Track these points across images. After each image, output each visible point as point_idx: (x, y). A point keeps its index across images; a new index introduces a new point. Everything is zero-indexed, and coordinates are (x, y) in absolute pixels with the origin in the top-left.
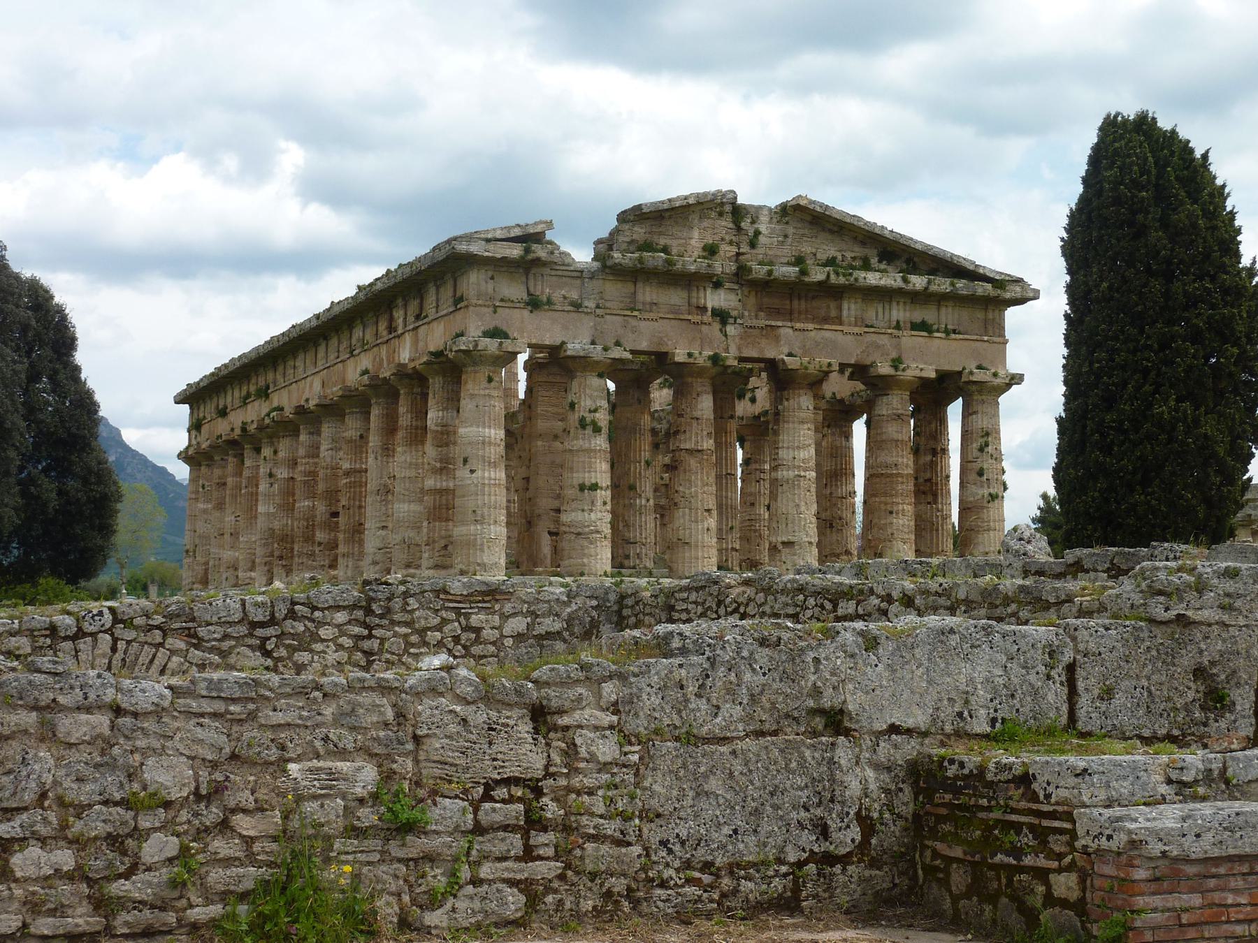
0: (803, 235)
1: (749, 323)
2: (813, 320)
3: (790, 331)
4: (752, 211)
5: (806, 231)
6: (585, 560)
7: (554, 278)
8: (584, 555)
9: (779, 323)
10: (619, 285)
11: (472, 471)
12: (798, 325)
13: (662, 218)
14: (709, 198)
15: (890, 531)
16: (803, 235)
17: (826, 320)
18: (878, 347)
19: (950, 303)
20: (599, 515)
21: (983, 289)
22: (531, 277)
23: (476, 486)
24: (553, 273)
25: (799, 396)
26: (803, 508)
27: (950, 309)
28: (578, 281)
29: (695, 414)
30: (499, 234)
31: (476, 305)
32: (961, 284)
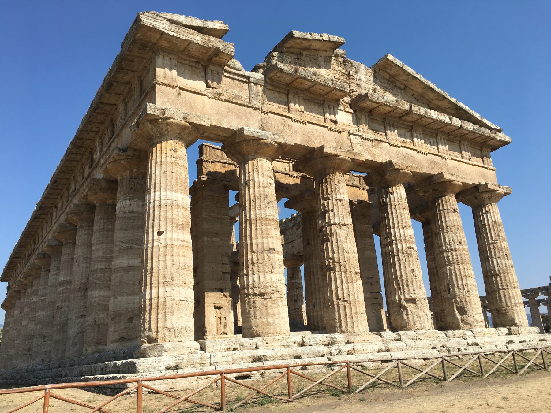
1: (364, 135)
6: (270, 320)
7: (228, 79)
8: (268, 314)
11: (160, 233)
18: (436, 164)
19: (465, 143)
21: (487, 132)
22: (209, 72)
23: (166, 247)
24: (226, 74)
26: (416, 272)
28: (246, 85)
29: (339, 197)
31: (162, 84)
32: (476, 127)
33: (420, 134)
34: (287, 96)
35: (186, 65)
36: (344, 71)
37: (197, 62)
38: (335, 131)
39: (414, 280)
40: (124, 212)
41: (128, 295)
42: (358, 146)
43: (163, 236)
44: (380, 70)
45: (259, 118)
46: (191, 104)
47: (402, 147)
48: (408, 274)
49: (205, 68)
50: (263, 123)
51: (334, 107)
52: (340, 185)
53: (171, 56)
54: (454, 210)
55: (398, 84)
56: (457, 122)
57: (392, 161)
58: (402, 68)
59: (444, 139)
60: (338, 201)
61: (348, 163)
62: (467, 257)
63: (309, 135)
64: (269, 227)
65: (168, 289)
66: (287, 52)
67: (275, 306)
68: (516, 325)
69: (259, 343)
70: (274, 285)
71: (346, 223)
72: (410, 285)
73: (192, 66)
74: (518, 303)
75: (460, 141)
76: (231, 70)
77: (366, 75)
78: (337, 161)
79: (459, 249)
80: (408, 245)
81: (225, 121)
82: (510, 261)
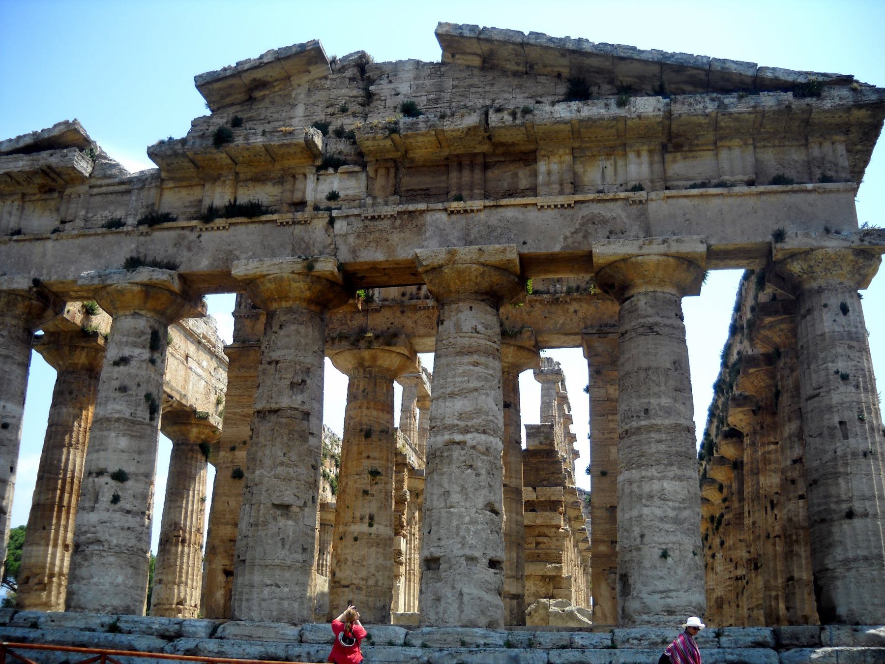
0: (471, 86)
3: (444, 216)
4: (387, 69)
5: (475, 80)
7: (98, 198)
9: (422, 206)
10: (184, 193)
12: (454, 205)
13: (251, 100)
14: (294, 50)
15: (637, 531)
16: (471, 86)
18: (605, 222)
19: (736, 142)
20: (105, 516)
24: (95, 191)
25: (459, 311)
26: (455, 497)
27: (737, 152)
33: (561, 163)
34: (204, 185)
35: (37, 200)
36: (355, 92)
37: (51, 190)
38: (294, 223)
39: (444, 515)
42: (351, 239)
44: (453, 56)
45: (133, 246)
46: (25, 259)
47: (485, 207)
48: (436, 503)
49: (61, 193)
50: (139, 252)
51: (305, 175)
52: (282, 333)
53: (12, 199)
54: (651, 328)
56: (647, 106)
57: (418, 251)
58: (479, 39)
59: (651, 152)
60: (274, 365)
61: (294, 285)
62: (653, 448)
63: (231, 248)
64: (106, 433)
66: (218, 109)
67: (86, 564)
70: (92, 529)
71: (274, 406)
72: (434, 528)
73: (45, 200)
74: (855, 559)
75: (715, 144)
76: (99, 183)
78: (268, 285)
79: (639, 429)
80: (447, 437)
81: (73, 269)
82: (852, 441)
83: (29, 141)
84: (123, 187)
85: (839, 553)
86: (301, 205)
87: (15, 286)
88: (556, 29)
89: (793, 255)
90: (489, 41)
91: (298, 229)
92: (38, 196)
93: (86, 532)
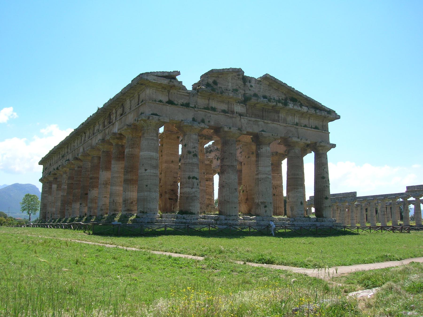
2: (270, 120)
3: (263, 123)
6: (190, 208)
11: (146, 170)
12: (266, 121)
17: (274, 121)
28: (188, 97)
30: (159, 74)
34: (209, 100)
40: (129, 154)
41: (131, 192)
43: (147, 171)
55: (274, 87)
58: (275, 81)
65: (148, 193)
68: (323, 217)
69: (185, 217)
76: (181, 91)
77: (255, 83)
83: (167, 74)
84: (187, 94)
85: (324, 205)
86: (233, 112)
87: (165, 121)
88: (290, 84)
89: (321, 146)
90: (277, 82)
91: (234, 119)
92: (160, 90)
93: (191, 194)
